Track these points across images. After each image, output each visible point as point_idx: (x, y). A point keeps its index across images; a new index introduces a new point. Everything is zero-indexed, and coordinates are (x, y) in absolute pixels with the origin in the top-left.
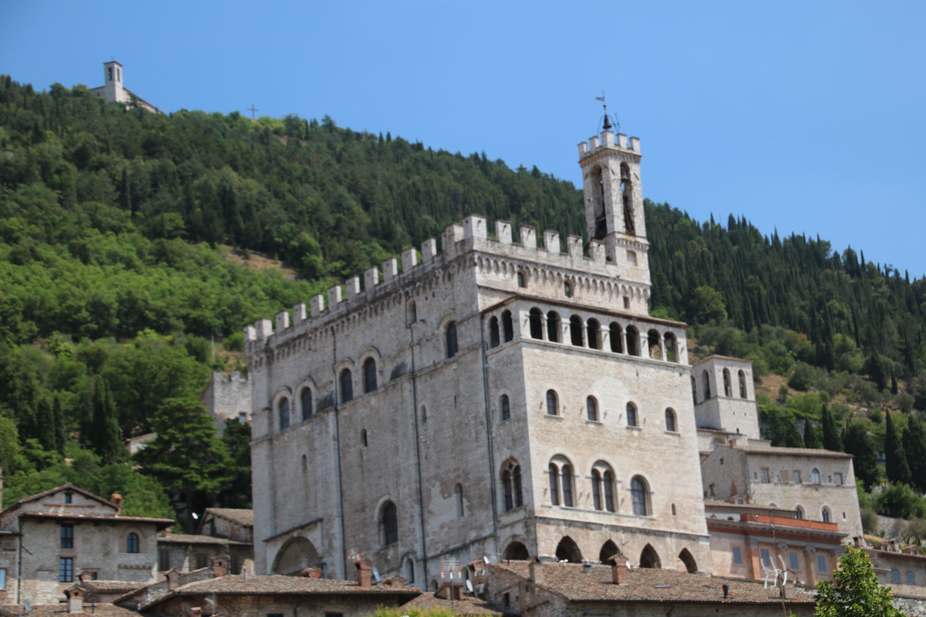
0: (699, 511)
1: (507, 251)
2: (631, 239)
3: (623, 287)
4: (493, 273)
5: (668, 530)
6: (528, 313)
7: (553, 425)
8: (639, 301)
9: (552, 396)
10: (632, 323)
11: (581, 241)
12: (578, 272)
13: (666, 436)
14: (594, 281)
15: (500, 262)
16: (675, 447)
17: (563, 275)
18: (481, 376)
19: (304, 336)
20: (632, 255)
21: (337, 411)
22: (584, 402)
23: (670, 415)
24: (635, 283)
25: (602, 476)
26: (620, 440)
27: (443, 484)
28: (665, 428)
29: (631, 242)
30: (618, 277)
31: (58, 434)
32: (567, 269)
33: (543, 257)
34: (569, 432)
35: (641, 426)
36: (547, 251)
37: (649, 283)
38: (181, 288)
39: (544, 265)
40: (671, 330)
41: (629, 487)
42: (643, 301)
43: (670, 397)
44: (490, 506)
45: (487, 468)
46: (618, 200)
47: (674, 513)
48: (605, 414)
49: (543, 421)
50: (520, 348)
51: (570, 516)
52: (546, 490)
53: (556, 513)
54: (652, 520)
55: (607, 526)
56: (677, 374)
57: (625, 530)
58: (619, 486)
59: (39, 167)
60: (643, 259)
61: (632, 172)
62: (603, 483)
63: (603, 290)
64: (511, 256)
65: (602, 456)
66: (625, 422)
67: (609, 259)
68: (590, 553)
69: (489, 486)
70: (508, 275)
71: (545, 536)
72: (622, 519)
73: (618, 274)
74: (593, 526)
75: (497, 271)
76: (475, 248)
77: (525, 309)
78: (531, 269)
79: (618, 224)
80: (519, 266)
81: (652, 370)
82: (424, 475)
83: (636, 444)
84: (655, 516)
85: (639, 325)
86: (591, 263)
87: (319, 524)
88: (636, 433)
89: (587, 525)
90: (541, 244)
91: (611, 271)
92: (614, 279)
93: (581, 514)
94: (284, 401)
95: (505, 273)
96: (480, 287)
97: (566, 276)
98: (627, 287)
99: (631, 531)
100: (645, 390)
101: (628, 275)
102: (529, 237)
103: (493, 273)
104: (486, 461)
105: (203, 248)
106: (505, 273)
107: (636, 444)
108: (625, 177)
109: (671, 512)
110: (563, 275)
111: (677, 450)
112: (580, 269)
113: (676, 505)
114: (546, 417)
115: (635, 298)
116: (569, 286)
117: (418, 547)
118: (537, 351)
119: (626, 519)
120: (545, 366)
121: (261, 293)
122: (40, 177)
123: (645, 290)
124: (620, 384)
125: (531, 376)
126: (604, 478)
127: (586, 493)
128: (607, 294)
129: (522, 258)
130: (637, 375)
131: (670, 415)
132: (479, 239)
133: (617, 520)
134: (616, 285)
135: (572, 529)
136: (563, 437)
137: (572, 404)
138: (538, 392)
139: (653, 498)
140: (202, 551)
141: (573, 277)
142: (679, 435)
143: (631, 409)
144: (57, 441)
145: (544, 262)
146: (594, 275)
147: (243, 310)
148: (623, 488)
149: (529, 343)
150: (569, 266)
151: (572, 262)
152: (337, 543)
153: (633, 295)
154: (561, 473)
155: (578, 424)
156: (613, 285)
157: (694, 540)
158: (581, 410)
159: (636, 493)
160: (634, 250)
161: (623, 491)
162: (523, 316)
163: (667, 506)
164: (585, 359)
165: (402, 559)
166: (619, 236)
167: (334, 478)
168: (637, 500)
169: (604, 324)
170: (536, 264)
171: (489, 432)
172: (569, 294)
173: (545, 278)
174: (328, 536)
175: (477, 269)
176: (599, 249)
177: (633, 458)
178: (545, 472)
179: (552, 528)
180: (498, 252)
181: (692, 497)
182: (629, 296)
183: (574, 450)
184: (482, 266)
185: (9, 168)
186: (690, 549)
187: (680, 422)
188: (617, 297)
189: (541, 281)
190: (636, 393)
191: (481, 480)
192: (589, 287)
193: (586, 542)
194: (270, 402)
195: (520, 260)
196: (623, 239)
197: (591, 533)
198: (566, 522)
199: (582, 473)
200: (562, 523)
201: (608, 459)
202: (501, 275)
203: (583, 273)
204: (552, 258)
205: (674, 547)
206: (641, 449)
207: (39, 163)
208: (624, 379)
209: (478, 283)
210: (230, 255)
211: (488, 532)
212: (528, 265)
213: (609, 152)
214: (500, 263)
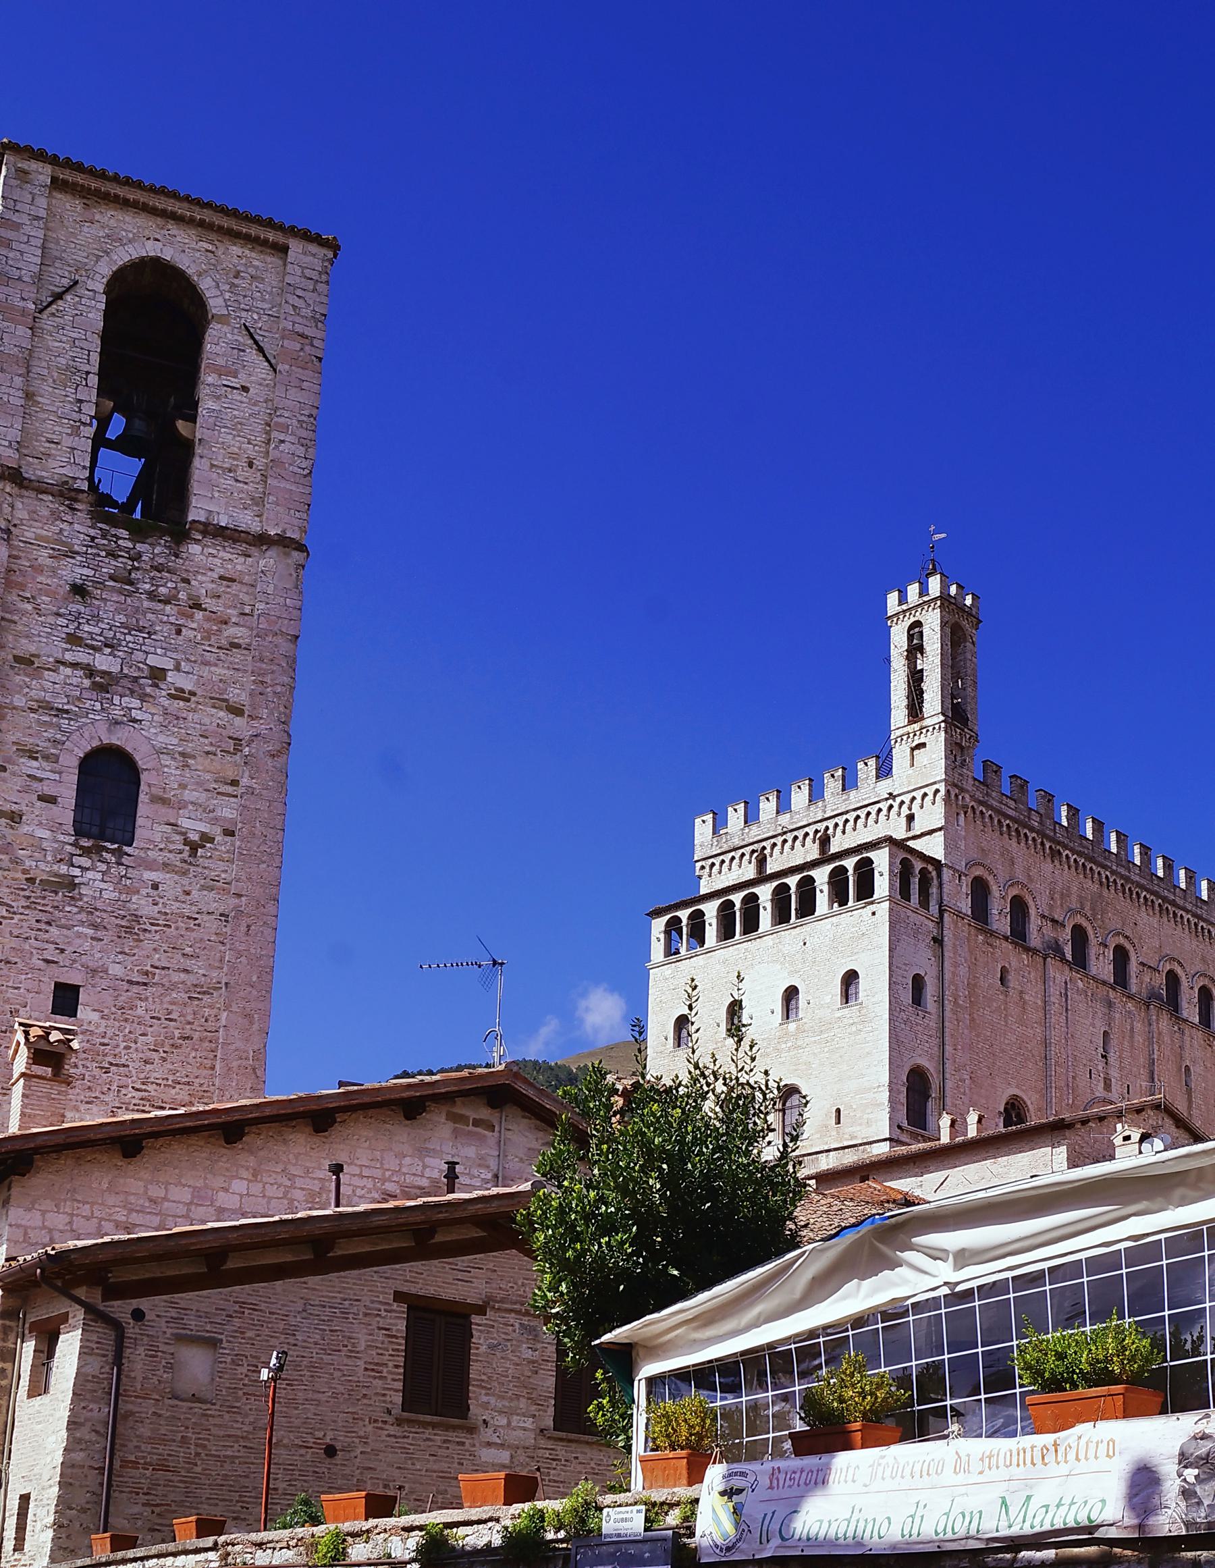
1: (737, 842)
2: (916, 726)
5: (826, 1148)
13: (839, 1014)
23: (850, 978)
61: (926, 631)
83: (789, 1044)
86: (853, 794)
88: (792, 1026)
92: (887, 799)
102: (768, 807)
107: (789, 1044)
109: (834, 1121)
111: (854, 1029)
143: (791, 994)
160: (922, 741)
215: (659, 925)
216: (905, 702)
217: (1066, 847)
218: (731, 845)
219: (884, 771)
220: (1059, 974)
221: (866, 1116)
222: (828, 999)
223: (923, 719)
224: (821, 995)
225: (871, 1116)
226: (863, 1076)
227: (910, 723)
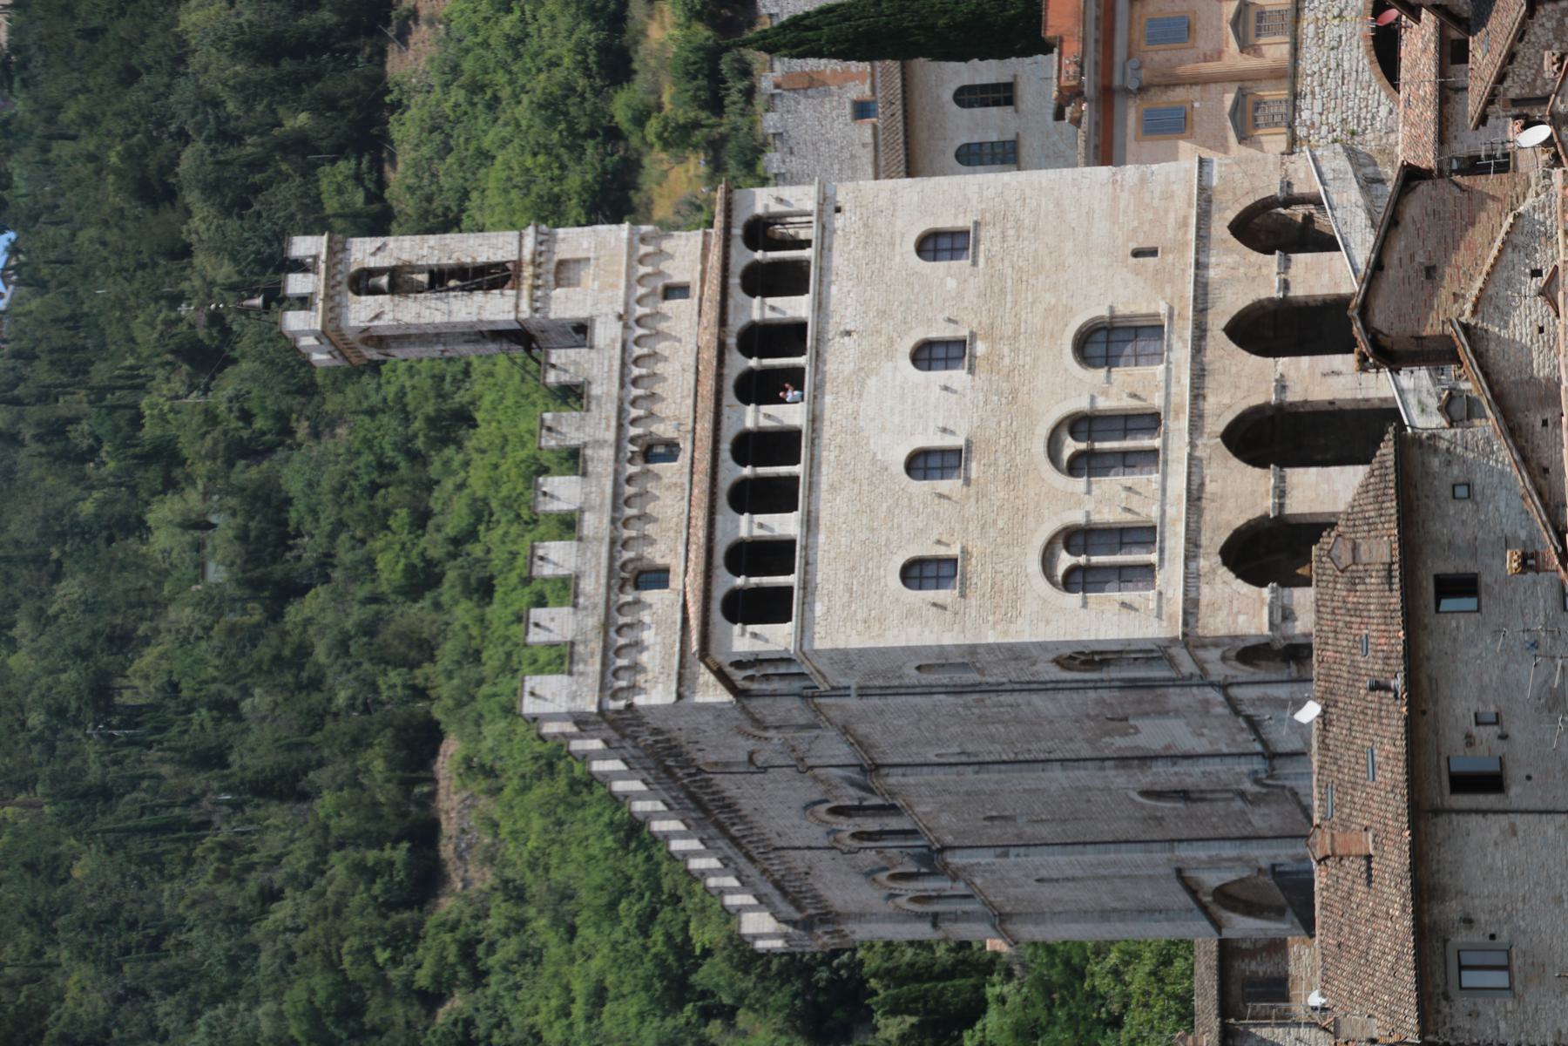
0: (1143, 180)
1: (593, 621)
2: (528, 271)
3: (639, 301)
4: (644, 658)
5: (1192, 271)
6: (737, 628)
7: (978, 572)
8: (671, 257)
9: (917, 573)
10: (732, 341)
11: (548, 416)
13: (981, 261)
14: (635, 382)
15: (617, 631)
16: (1004, 238)
17: (631, 469)
18: (875, 701)
19: (778, 885)
20: (564, 272)
21: (944, 849)
22: (922, 488)
23: (934, 245)
24: (629, 267)
25: (1082, 446)
26: (1000, 394)
27: (1108, 733)
28: (963, 264)
29: (537, 276)
30: (620, 317)
31: (948, 973)
32: (617, 459)
33: (596, 524)
34: (992, 533)
35: (963, 332)
36: (582, 511)
37: (626, 226)
38: (474, 30)
39: (613, 521)
40: (737, 231)
41: (1102, 372)
42: (667, 245)
43: (892, 244)
44: (1159, 691)
45: (1075, 695)
46: (441, 305)
47: (1153, 252)
48: (944, 430)
49: (973, 600)
50: (817, 652)
51: (1175, 541)
52: (1123, 604)
53: (1171, 577)
54: (1171, 317)
55: (1192, 445)
56: (839, 221)
57: (1197, 395)
58: (1103, 404)
59: (241, 464)
60: (574, 240)
62: (1097, 445)
63: (654, 356)
64: (601, 610)
65: (1039, 447)
66: (957, 377)
67: (581, 331)
68: (1253, 492)
69: (1116, 693)
70: (646, 617)
71: (1222, 614)
72: (1174, 399)
73: (612, 318)
74: (1196, 480)
75: (637, 645)
76: (593, 708)
77: (730, 635)
78: (628, 555)
79: (496, 308)
80: (621, 589)
81: (834, 289)
82: (1086, 752)
83: (1006, 350)
84: (1162, 309)
85: (737, 323)
86: (595, 390)
87: (1188, 874)
88: (981, 348)
89: (1195, 498)
90: (568, 525)
91: (607, 333)
92: (626, 327)
93: (1171, 512)
94: (915, 900)
95: (640, 624)
96: (680, 696)
97: (631, 461)
98: (641, 291)
99: (1199, 375)
100: (882, 314)
101: (614, 286)
103: (644, 658)
104: (1061, 696)
105: (405, 131)
106: (640, 624)
107: (1006, 350)
108: (384, 281)
109: (1150, 260)
110: (631, 469)
111: (1011, 232)
112: (614, 423)
113: (1133, 245)
114: (963, 595)
115: (665, 266)
116: (656, 451)
117: (1244, 767)
118: (819, 609)
119: (1173, 390)
120: (850, 591)
121: (508, 22)
122: (265, 465)
123: (643, 240)
124: (872, 382)
125: (876, 630)
126: (1092, 444)
127: (1124, 494)
128: (663, 347)
129: (603, 581)
130: (848, 333)
131: (934, 245)
132: (573, 697)
133: (1177, 417)
134: (638, 322)
135: (1204, 541)
136: (1002, 550)
137: (928, 519)
138: (909, 613)
139: (1122, 310)
140: (1235, 990)
141: (633, 440)
142: (977, 224)
143: (928, 355)
144: (964, 975)
145: (606, 520)
146: (622, 385)
147: (558, 92)
148: (1105, 393)
149: (803, 631)
150: (608, 453)
151: (599, 444)
152: (1229, 851)
153: (659, 274)
154: (1082, 560)
155: (971, 508)
156: (639, 331)
157: (1209, 201)
158: (941, 496)
159: (1114, 350)
160: (552, 266)
161: (1114, 389)
162: (743, 640)
164: (826, 476)
165: (1268, 786)
166: (525, 311)
167: (1090, 856)
168: (1129, 350)
169: (742, 419)
170: (613, 542)
171: (997, 689)
172: (670, 450)
173: (643, 517)
174: (1214, 864)
175: (640, 701)
176: (565, 363)
177: (1036, 359)
178: (1085, 605)
179: (1206, 593)
180: (596, 645)
181: (1115, 199)
182: (660, 285)
184: (633, 688)
185: (253, 534)
186: (1231, 215)
187: (946, 222)
188: (665, 317)
189: (650, 529)
190: (891, 340)
191: (1101, 702)
192: (652, 396)
193: (1231, 504)
194: (920, 916)
195: (609, 587)
196: (531, 296)
197: (1210, 487)
198: (1190, 556)
199: (1079, 503)
200: (1193, 565)
202: (648, 636)
203: (621, 412)
204: (595, 499)
205: (1230, 260)
206: (1015, 336)
207: (230, 464)
208: (862, 372)
209: (672, 698)
210: (411, 55)
211: (1215, 695)
212: (618, 564)
213: (331, 326)
214: (621, 641)
216: (479, 296)
218: (592, 635)
221: (1156, 202)
222: (951, 283)
223: (518, 264)
224: (947, 298)
225: (1157, 194)
226: (1090, 213)
227: (517, 287)
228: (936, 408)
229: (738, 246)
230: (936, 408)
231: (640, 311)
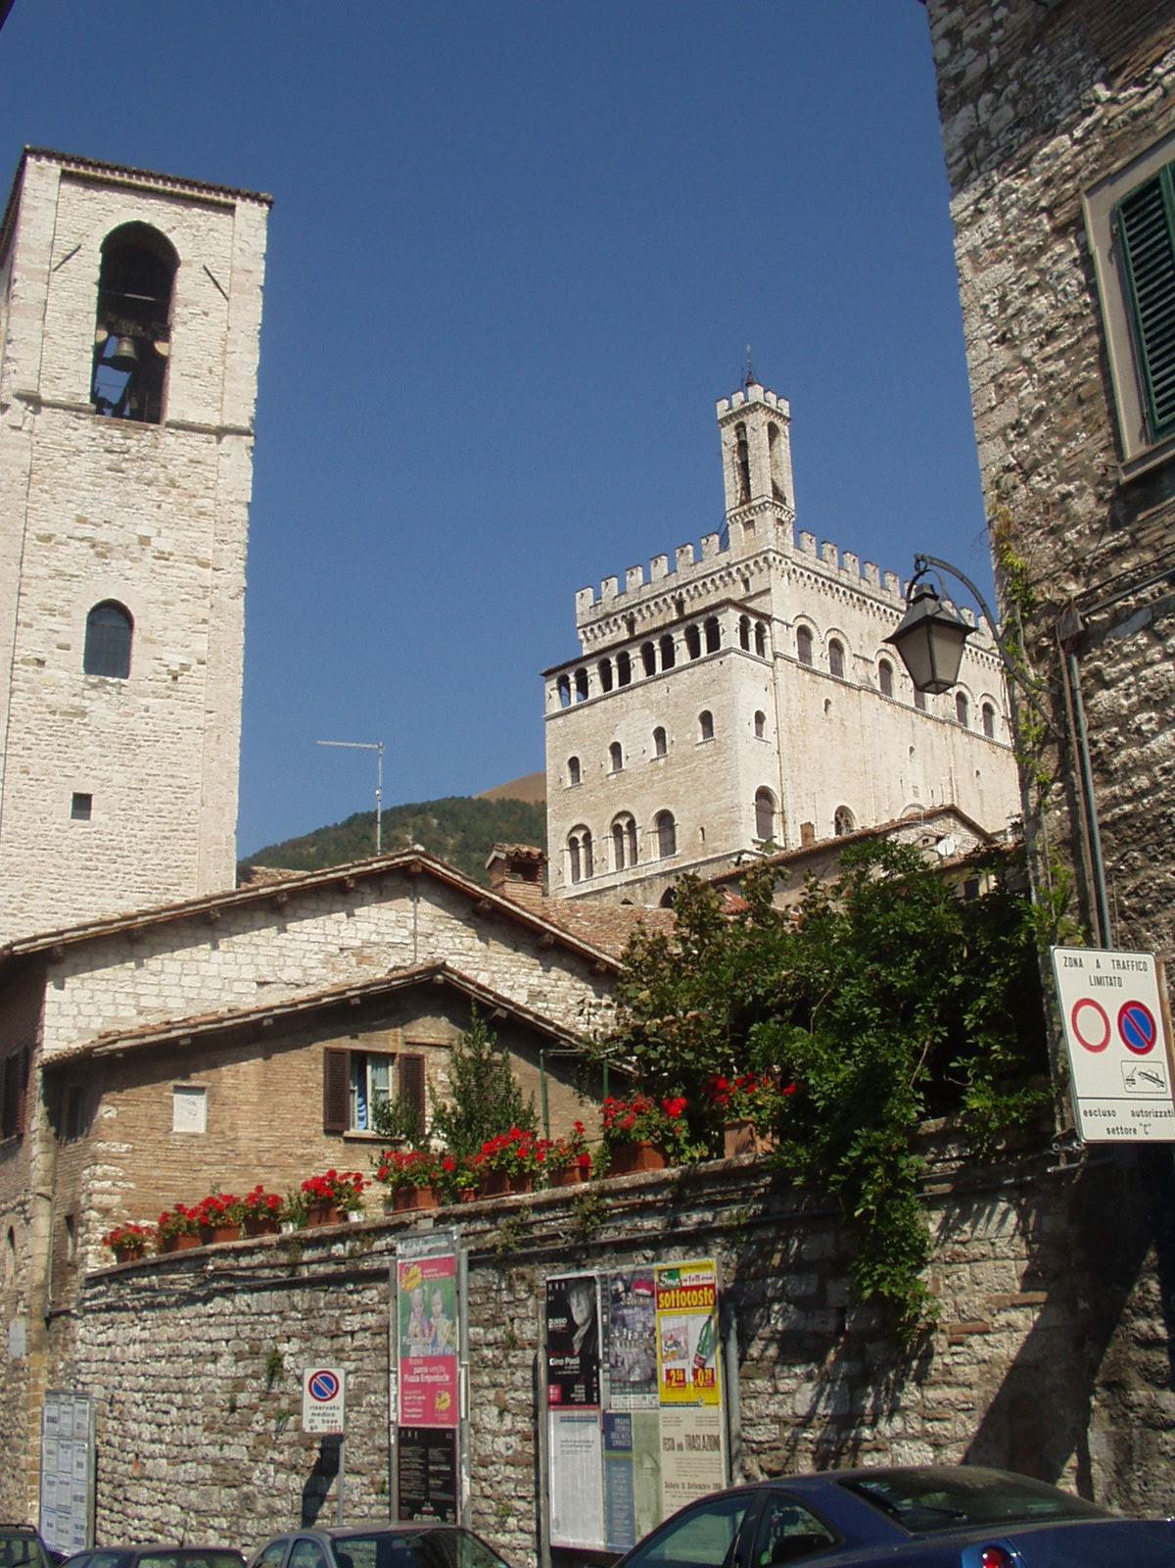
1: (609, 609)
12: (685, 585)
23: (706, 718)
93: (596, 882)
143: (660, 734)
163: (695, 833)
183: (592, 813)
201: (627, 807)
206: (666, 778)
215: (554, 683)
217: (870, 597)
219: (724, 545)
220: (872, 703)
228: (639, 748)
229: (704, 617)
230: (639, 748)
231: (733, 570)
